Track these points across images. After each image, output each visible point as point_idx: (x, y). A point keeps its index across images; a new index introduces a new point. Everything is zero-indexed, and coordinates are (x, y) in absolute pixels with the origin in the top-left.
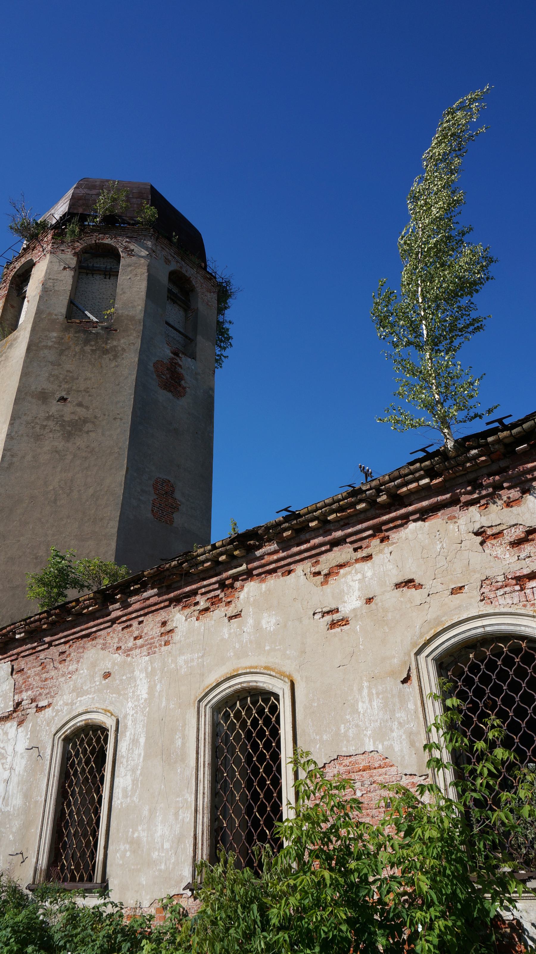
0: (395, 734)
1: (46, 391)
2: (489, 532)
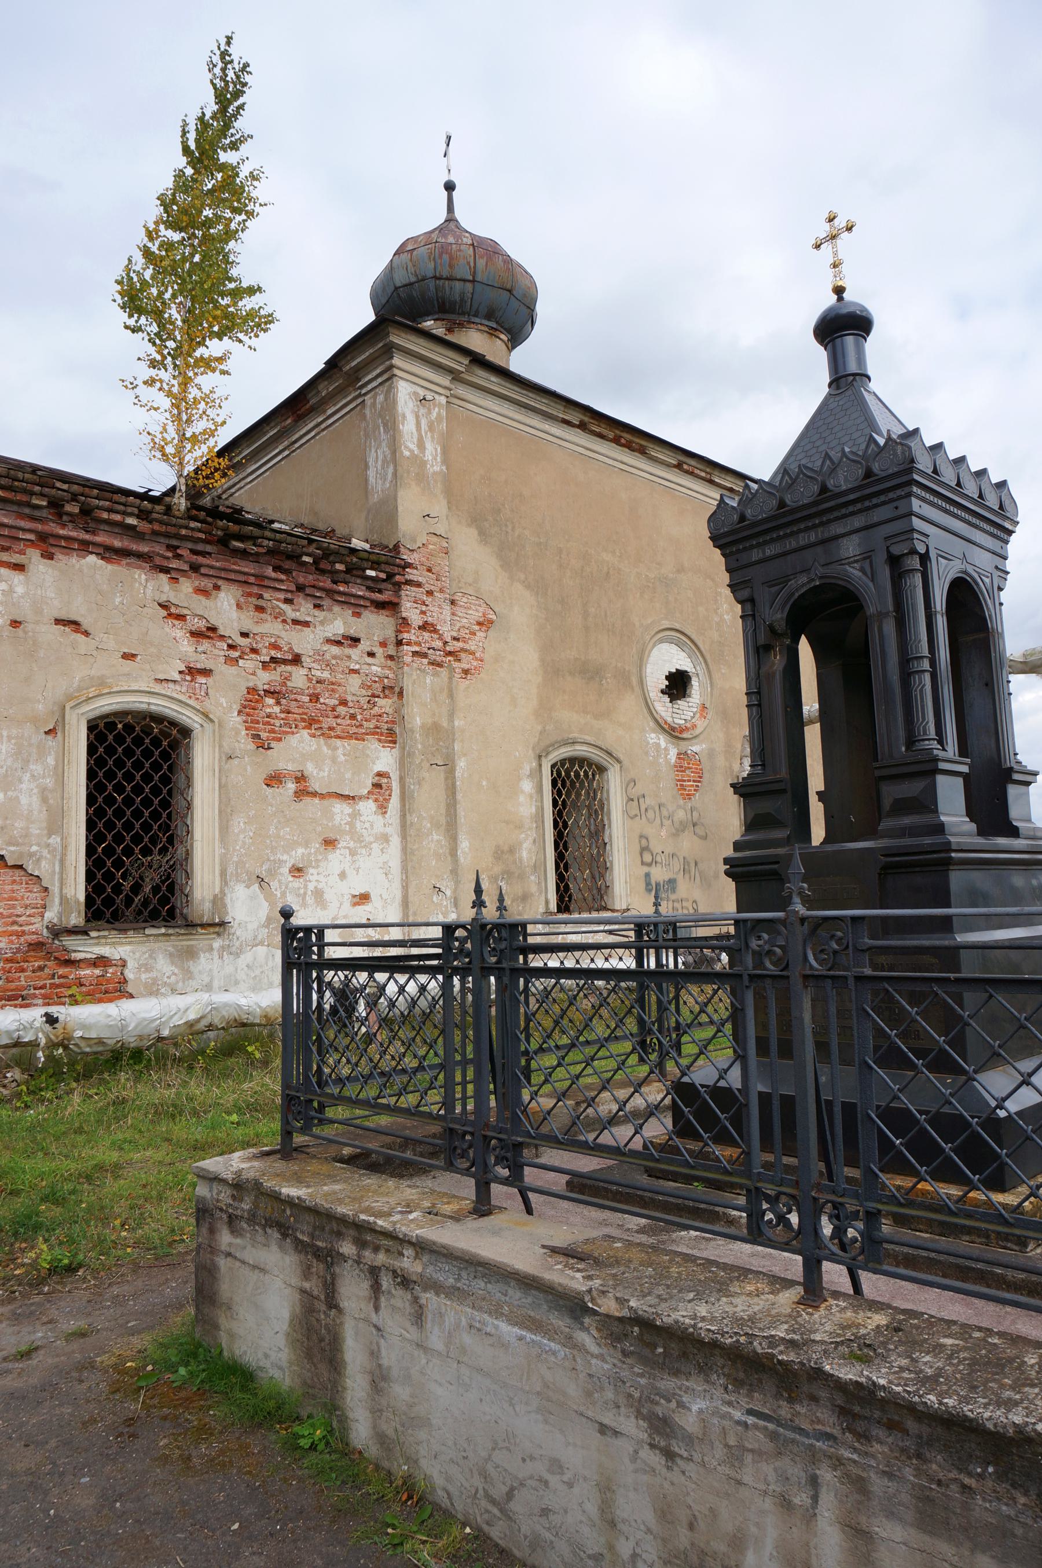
0: (24, 786)
2: (173, 610)
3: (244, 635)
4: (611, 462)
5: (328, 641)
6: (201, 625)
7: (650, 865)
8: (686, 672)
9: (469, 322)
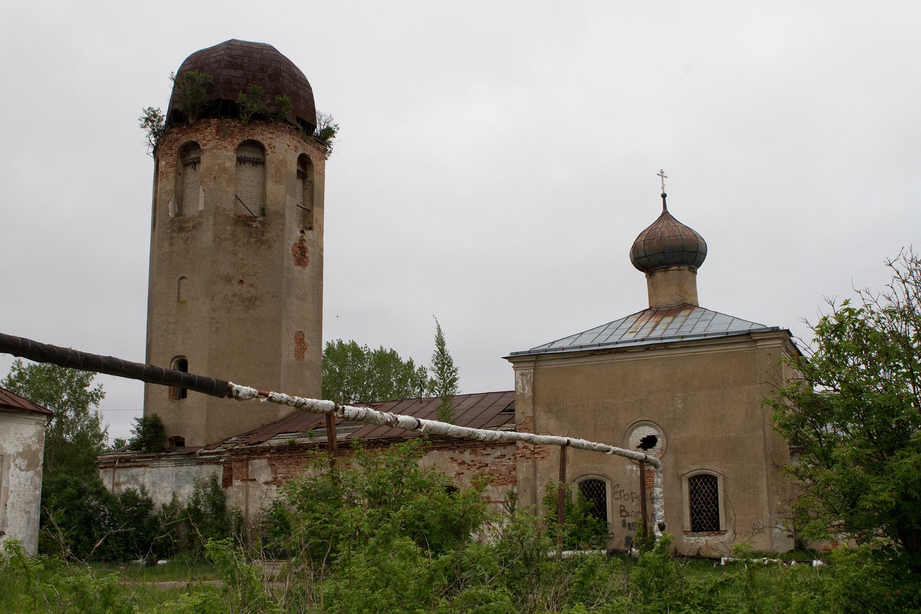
1: (230, 275)
3: (472, 461)
4: (611, 361)
5: (496, 458)
6: (460, 461)
7: (626, 516)
8: (654, 436)
9: (656, 270)
